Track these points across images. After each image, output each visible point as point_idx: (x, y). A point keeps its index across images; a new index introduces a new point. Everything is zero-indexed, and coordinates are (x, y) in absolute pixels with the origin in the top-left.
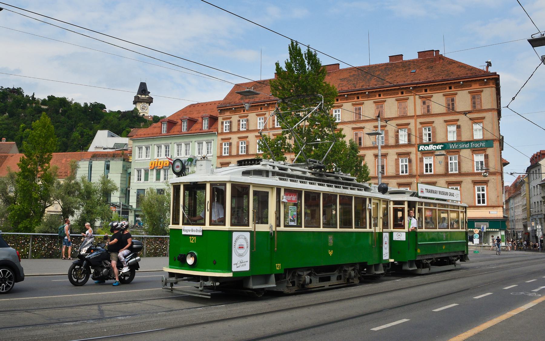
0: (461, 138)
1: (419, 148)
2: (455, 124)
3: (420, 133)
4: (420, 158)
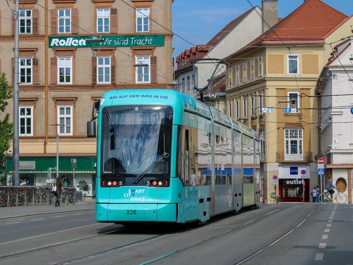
1: (50, 42)
2: (109, 7)
3: (52, 18)
4: (52, 59)
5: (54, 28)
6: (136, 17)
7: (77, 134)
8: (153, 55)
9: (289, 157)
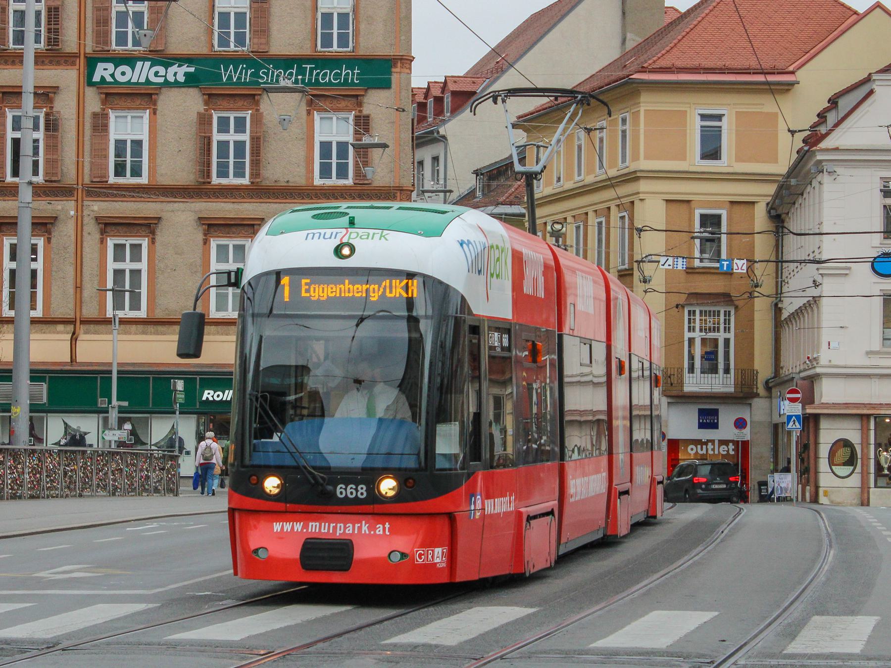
0: (268, 43)
3: (98, 9)
4: (95, 115)
5: (102, 36)
6: (319, 10)
7: (159, 314)
8: (360, 111)
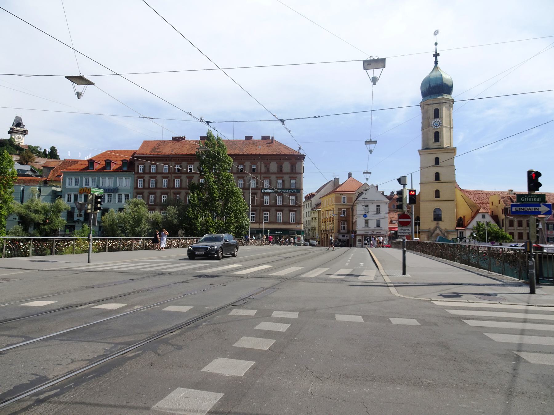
9: (342, 231)
